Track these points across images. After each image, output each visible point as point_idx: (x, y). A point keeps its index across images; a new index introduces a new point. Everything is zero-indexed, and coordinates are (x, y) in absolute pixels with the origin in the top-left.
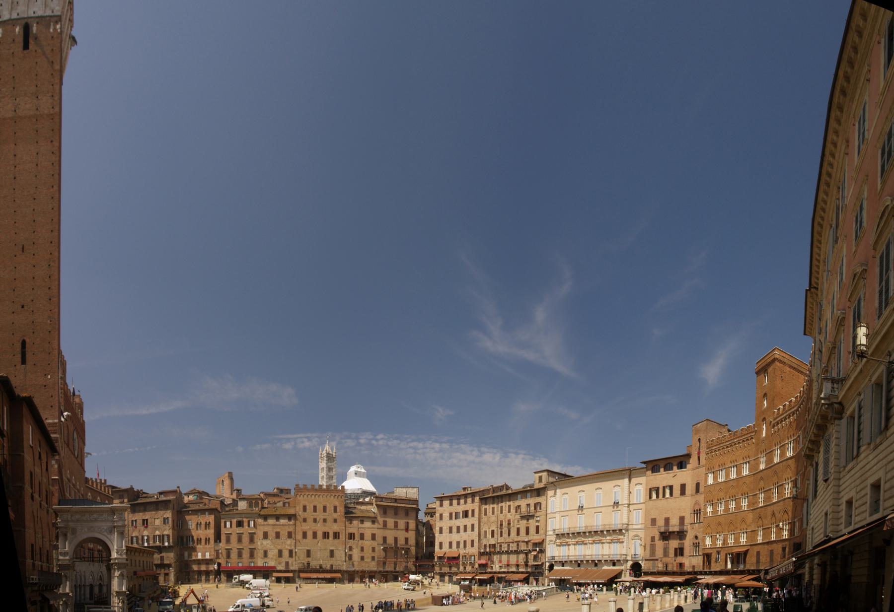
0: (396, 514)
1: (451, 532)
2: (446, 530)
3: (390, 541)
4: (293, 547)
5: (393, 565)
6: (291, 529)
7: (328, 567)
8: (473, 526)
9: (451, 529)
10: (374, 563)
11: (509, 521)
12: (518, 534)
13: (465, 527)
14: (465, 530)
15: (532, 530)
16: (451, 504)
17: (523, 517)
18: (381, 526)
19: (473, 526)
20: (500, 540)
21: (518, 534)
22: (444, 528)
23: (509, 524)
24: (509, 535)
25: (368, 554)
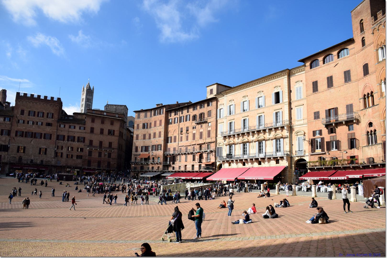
0: (103, 123)
1: (144, 138)
2: (141, 137)
3: (96, 143)
4: (7, 143)
5: (96, 164)
6: (8, 128)
7: (38, 162)
8: (160, 133)
9: (144, 135)
10: (79, 161)
11: (187, 128)
12: (194, 138)
13: (155, 134)
14: (154, 137)
15: (205, 135)
16: (146, 116)
17: (198, 124)
19: (160, 133)
20: (181, 144)
21: (194, 138)
22: (140, 135)
23: (187, 130)
24: (187, 140)
25: (75, 153)
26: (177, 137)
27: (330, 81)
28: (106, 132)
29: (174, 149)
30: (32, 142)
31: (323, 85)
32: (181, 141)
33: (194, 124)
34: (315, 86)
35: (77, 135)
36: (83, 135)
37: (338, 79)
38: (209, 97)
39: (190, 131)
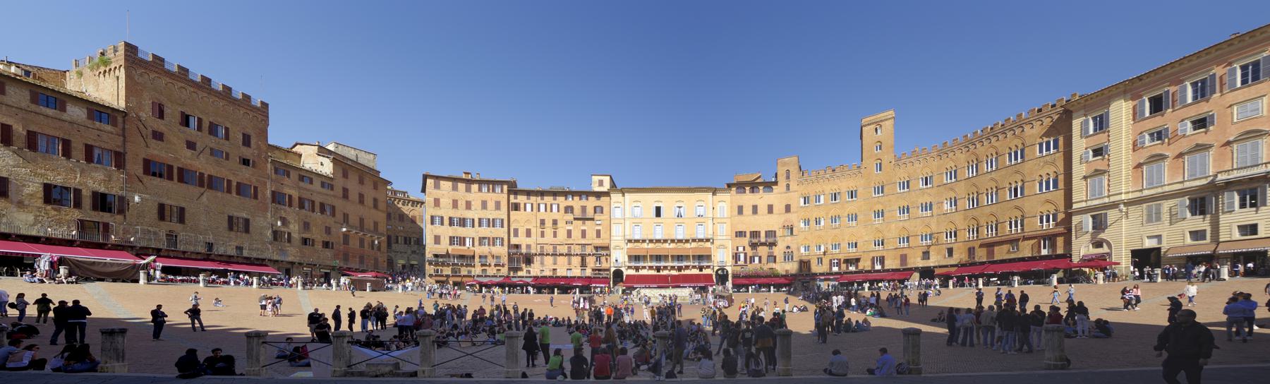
15: (591, 234)
18: (340, 193)
20: (541, 240)
26: (533, 231)
27: (755, 209)
28: (369, 201)
29: (528, 246)
30: (204, 198)
31: (748, 210)
32: (543, 235)
33: (570, 217)
34: (740, 210)
35: (318, 200)
36: (329, 201)
37: (763, 209)
38: (597, 189)
39: (559, 225)
